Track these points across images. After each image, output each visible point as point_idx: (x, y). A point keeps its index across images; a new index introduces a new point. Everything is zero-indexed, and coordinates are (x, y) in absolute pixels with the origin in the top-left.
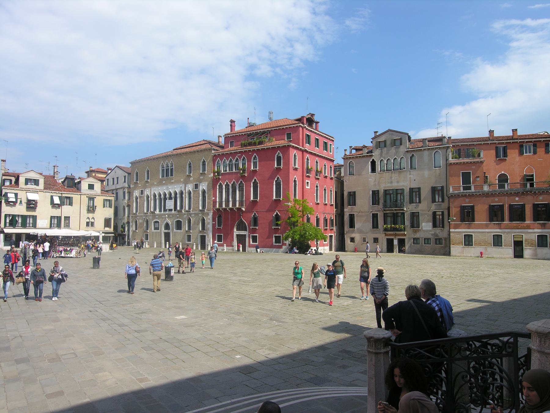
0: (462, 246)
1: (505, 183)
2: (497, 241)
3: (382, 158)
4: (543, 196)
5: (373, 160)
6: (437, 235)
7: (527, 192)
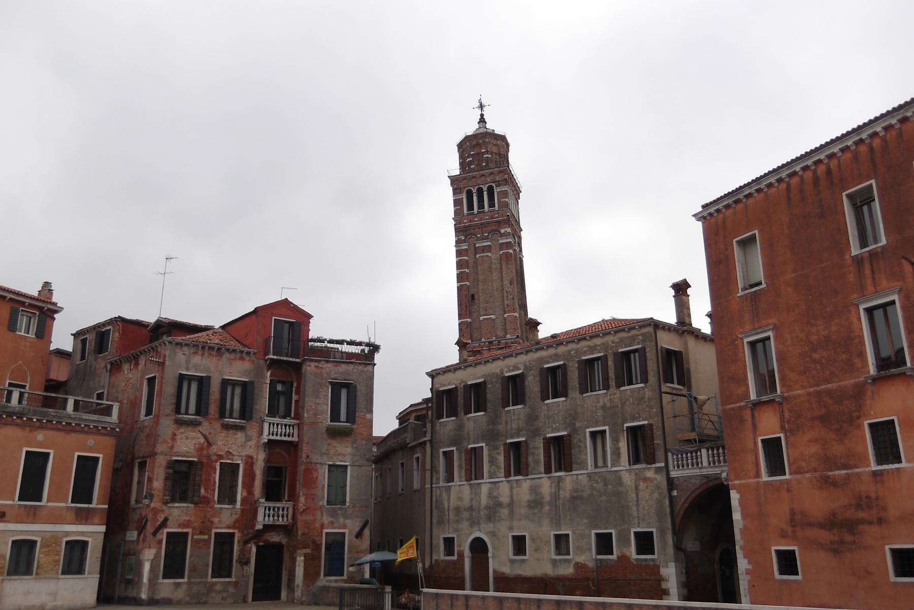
7: (10, 415)
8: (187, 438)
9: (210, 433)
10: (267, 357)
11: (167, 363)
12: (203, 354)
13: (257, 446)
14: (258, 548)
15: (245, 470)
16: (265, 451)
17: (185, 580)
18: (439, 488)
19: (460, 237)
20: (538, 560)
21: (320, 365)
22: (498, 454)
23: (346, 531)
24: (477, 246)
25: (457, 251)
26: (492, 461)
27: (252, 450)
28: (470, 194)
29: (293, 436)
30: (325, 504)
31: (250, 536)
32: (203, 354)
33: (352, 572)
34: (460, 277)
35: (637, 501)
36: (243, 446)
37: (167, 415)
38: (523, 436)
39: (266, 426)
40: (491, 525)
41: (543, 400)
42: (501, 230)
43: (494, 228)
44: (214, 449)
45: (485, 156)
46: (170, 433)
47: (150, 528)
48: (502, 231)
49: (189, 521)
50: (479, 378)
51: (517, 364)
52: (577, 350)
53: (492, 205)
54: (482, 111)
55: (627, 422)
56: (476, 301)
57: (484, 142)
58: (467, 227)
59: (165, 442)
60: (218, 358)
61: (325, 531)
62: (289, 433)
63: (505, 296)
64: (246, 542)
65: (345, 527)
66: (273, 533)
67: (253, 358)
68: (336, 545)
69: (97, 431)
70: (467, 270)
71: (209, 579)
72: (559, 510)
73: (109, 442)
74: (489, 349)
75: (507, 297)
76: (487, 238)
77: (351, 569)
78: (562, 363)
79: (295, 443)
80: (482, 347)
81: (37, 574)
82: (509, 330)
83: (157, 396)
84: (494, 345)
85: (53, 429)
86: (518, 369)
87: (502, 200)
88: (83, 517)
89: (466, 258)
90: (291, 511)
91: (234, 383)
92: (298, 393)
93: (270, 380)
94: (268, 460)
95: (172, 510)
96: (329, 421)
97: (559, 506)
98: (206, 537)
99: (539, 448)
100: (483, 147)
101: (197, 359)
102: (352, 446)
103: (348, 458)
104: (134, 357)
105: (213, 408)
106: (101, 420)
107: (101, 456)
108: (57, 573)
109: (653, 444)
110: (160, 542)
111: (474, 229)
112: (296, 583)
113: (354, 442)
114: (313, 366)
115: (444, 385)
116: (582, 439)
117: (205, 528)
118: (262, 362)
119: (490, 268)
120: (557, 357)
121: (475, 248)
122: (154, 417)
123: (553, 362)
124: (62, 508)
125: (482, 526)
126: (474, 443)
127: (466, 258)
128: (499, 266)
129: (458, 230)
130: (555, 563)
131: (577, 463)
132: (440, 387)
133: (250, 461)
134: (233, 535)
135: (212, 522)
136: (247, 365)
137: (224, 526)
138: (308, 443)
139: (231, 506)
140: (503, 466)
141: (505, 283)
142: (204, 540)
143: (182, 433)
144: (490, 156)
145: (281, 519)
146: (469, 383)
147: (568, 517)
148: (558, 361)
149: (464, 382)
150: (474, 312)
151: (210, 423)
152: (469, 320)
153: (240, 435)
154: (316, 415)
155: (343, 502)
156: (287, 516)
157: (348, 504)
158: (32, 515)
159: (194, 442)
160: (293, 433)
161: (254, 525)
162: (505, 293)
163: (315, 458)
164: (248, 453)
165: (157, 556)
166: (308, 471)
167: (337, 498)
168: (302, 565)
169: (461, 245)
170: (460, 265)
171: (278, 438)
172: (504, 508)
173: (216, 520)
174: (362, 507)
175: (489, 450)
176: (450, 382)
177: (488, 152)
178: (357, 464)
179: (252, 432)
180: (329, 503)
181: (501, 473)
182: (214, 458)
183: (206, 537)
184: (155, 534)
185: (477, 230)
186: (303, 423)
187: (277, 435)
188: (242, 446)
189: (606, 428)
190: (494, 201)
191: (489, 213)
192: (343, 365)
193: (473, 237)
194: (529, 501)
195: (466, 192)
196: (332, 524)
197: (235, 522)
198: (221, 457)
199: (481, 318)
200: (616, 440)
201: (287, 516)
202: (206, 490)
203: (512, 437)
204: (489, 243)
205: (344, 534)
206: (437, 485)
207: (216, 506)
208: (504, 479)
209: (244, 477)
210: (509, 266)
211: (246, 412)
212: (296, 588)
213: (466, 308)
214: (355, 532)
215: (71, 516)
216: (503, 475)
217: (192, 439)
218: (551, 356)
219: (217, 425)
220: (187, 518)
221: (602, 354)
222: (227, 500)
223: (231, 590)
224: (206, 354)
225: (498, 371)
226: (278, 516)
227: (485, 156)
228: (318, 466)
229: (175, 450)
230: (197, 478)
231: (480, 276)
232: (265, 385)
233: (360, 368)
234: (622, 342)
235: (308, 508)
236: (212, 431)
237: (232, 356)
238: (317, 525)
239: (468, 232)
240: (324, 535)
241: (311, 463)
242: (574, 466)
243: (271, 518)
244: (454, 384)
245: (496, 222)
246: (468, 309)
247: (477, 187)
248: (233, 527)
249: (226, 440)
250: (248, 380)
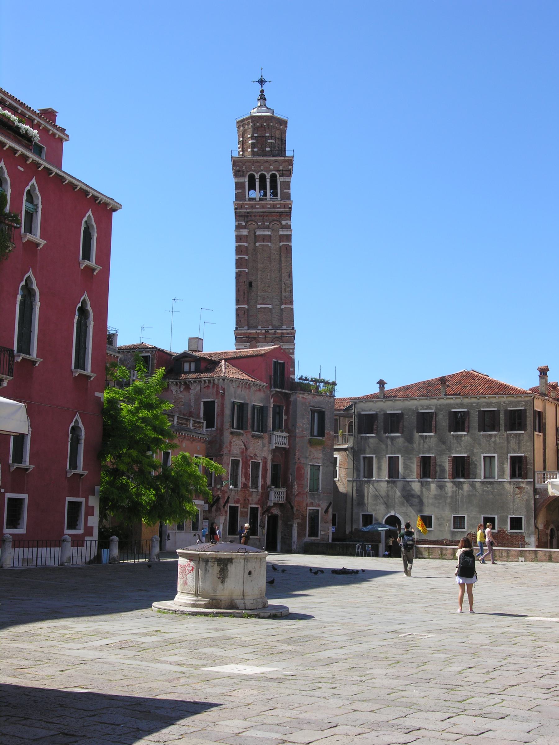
8: (236, 445)
9: (246, 442)
10: (272, 389)
11: (226, 393)
13: (268, 450)
14: (269, 517)
15: (263, 466)
18: (360, 481)
19: (240, 222)
20: (440, 531)
22: (412, 463)
23: (319, 508)
24: (258, 233)
25: (237, 236)
26: (406, 467)
28: (252, 179)
34: (239, 263)
35: (514, 500)
38: (432, 453)
40: (404, 508)
41: (450, 431)
42: (282, 222)
43: (275, 218)
45: (269, 141)
47: (222, 502)
48: (284, 223)
49: (238, 499)
50: (397, 410)
51: (430, 405)
52: (478, 404)
53: (275, 194)
54: (262, 87)
55: (510, 453)
56: (253, 289)
57: (268, 125)
58: (249, 213)
63: (283, 287)
65: (319, 506)
70: (246, 257)
72: (459, 501)
74: (265, 337)
75: (285, 290)
76: (267, 228)
77: (322, 533)
78: (466, 410)
79: (287, 449)
80: (258, 334)
82: (285, 321)
83: (218, 415)
84: (270, 334)
86: (430, 409)
87: (285, 191)
89: (246, 244)
90: (285, 494)
92: (287, 413)
94: (273, 460)
97: (458, 499)
98: (246, 510)
99: (445, 462)
100: (267, 130)
103: (320, 461)
104: (185, 383)
109: (527, 468)
110: (226, 512)
111: (255, 216)
112: (293, 541)
114: (301, 397)
115: (365, 411)
116: (478, 460)
118: (269, 392)
119: (270, 258)
120: (461, 405)
121: (255, 236)
122: (217, 429)
123: (459, 409)
125: (396, 508)
126: (391, 454)
127: (246, 244)
128: (278, 257)
129: (239, 216)
130: (453, 533)
131: (473, 474)
132: (362, 411)
134: (257, 508)
135: (248, 500)
136: (261, 395)
137: (254, 503)
138: (299, 450)
140: (415, 471)
141: (283, 275)
144: (274, 141)
146: (388, 412)
147: (465, 506)
148: (463, 408)
149: (383, 411)
150: (251, 299)
151: (246, 435)
152: (246, 307)
153: (260, 442)
155: (317, 490)
157: (321, 492)
159: (239, 447)
161: (267, 503)
162: (283, 285)
163: (303, 460)
165: (225, 520)
166: (299, 469)
168: (296, 529)
169: (241, 230)
170: (239, 251)
171: (280, 446)
172: (415, 498)
173: (250, 499)
174: (328, 493)
175: (404, 460)
176: (371, 409)
177: (272, 137)
178: (325, 465)
181: (413, 475)
182: (249, 458)
183: (246, 510)
184: (224, 507)
185: (258, 218)
186: (295, 436)
189: (496, 455)
190: (277, 190)
191: (271, 202)
193: (253, 223)
194: (435, 495)
195: (249, 177)
196: (312, 504)
197: (259, 501)
198: (252, 458)
199: (259, 306)
200: (501, 463)
203: (423, 453)
204: (269, 233)
205: (318, 510)
206: (358, 479)
208: (416, 480)
210: (288, 259)
211: (262, 428)
212: (293, 544)
213: (244, 295)
214: (324, 510)
216: (415, 477)
218: (457, 404)
219: (250, 436)
220: (238, 497)
221: (496, 409)
224: (243, 387)
225: (414, 407)
227: (269, 141)
231: (259, 265)
234: (511, 403)
239: (249, 219)
240: (308, 510)
242: (471, 476)
244: (374, 411)
245: (277, 213)
246: (245, 296)
247: (260, 173)
250: (262, 405)
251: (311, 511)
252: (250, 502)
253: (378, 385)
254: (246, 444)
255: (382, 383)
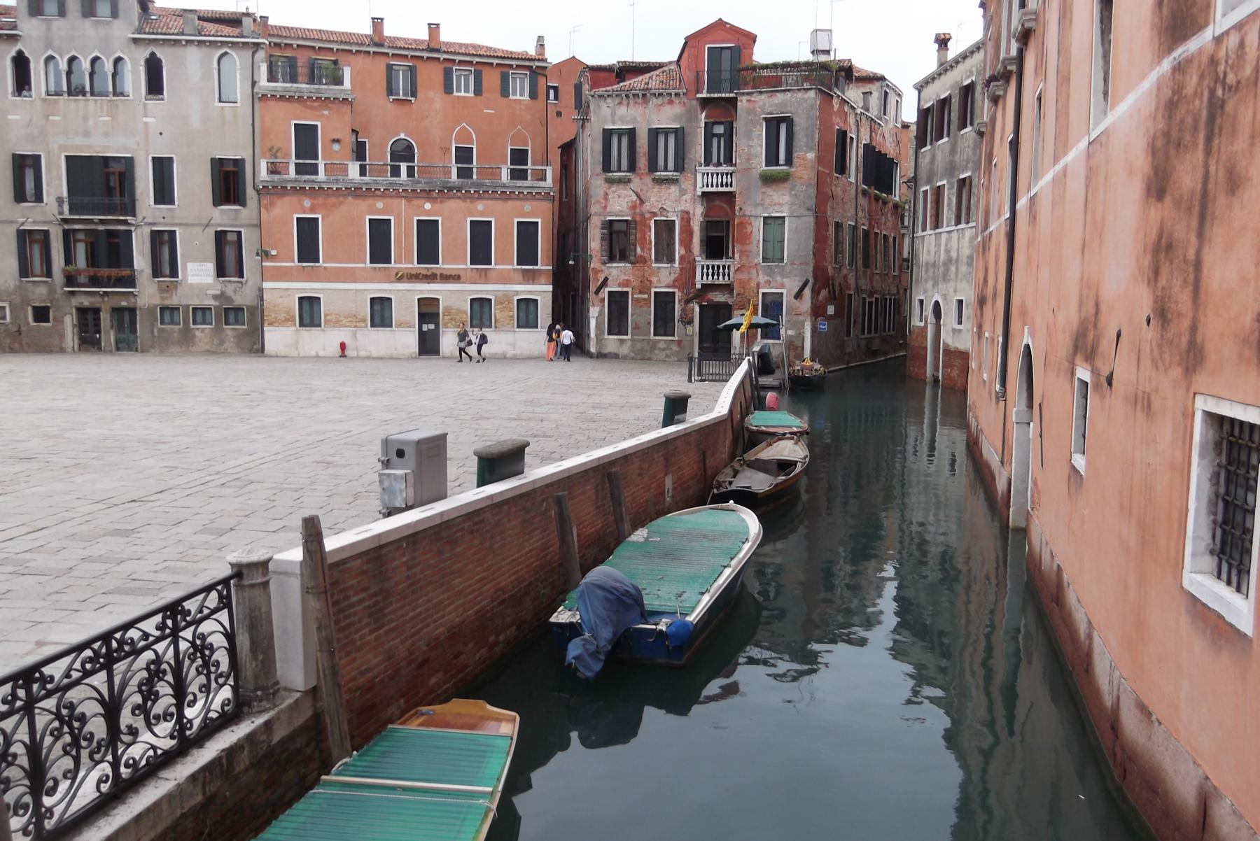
0: (294, 328)
1: (401, 164)
2: (381, 312)
3: (50, 52)
4: (486, 202)
5: (20, 53)
6: (229, 299)
7: (450, 189)
8: (619, 197)
9: (641, 190)
11: (592, 119)
12: (628, 104)
14: (701, 307)
15: (681, 227)
16: (702, 205)
17: (629, 337)
21: (753, 99)
27: (688, 205)
29: (731, 186)
30: (761, 261)
31: (691, 295)
32: (628, 104)
33: (791, 336)
36: (678, 201)
37: (597, 175)
39: (699, 176)
44: (647, 206)
46: (602, 193)
47: (593, 288)
49: (627, 280)
59: (598, 202)
60: (645, 105)
61: (761, 291)
62: (727, 183)
64: (688, 301)
65: (782, 286)
66: (717, 293)
67: (684, 99)
68: (773, 306)
69: (531, 196)
71: (652, 337)
73: (546, 207)
81: (495, 327)
85: (488, 199)
88: (530, 277)
91: (666, 132)
93: (706, 123)
94: (706, 214)
95: (611, 270)
96: (764, 165)
98: (646, 296)
101: (622, 110)
102: (790, 193)
105: (642, 162)
106: (535, 185)
107: (539, 220)
108: (513, 327)
113: (792, 189)
114: (744, 101)
117: (644, 289)
118: (694, 102)
124: (509, 270)
133: (686, 216)
134: (674, 293)
135: (650, 281)
138: (740, 193)
139: (669, 265)
142: (644, 299)
143: (614, 192)
145: (721, 277)
151: (641, 179)
153: (674, 189)
154: (749, 159)
155: (782, 260)
156: (729, 275)
157: (785, 262)
158: (484, 277)
159: (626, 200)
160: (731, 183)
163: (749, 210)
164: (683, 208)
165: (601, 313)
166: (743, 225)
167: (773, 255)
171: (714, 189)
173: (654, 279)
174: (801, 264)
178: (795, 214)
179: (686, 185)
180: (765, 260)
182: (647, 215)
183: (646, 296)
184: (597, 292)
187: (712, 186)
188: (676, 201)
192: (778, 94)
197: (674, 281)
198: (654, 214)
201: (729, 275)
202: (642, 249)
207: (654, 265)
209: (680, 234)
215: (519, 277)
217: (624, 198)
219: (648, 180)
220: (626, 278)
222: (665, 259)
223: (675, 348)
226: (718, 275)
228: (752, 219)
229: (608, 210)
230: (632, 237)
232: (699, 130)
233: (800, 95)
235: (743, 266)
236: (644, 188)
237: (660, 101)
238: (753, 285)
241: (745, 216)
243: (710, 277)
248: (674, 286)
249: (660, 197)
251: (769, 299)
252: (655, 284)
253: (936, 46)
254: (641, 194)
255: (943, 42)
